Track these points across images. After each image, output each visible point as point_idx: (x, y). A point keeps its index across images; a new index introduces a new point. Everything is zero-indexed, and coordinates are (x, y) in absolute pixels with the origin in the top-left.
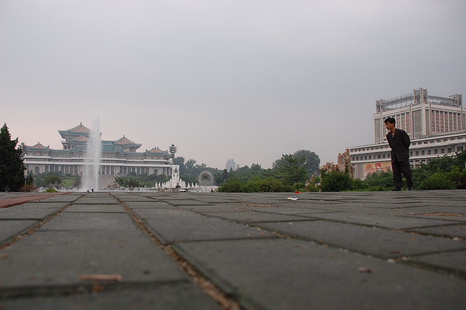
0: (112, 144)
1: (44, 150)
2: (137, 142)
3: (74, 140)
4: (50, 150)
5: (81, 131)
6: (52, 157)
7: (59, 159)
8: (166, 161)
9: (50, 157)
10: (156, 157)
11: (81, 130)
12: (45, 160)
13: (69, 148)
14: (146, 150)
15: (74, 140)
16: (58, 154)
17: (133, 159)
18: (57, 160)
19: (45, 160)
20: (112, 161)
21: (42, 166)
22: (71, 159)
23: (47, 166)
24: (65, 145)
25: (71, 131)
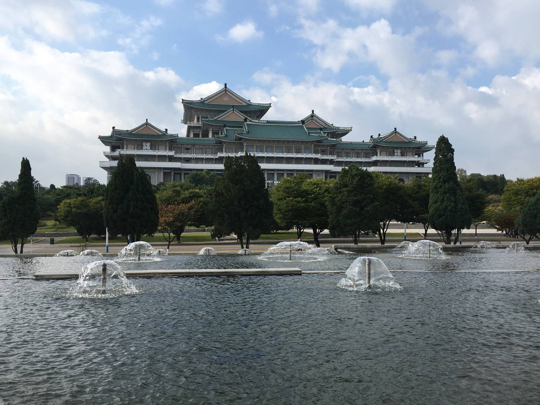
0: (301, 124)
1: (158, 136)
2: (339, 123)
3: (216, 118)
4: (171, 135)
5: (226, 100)
6: (176, 153)
7: (191, 158)
8: (416, 158)
9: (172, 153)
10: (399, 151)
11: (226, 99)
12: (161, 158)
13: (206, 135)
14: (372, 137)
15: (216, 118)
16: (189, 146)
17: (358, 157)
18: (188, 160)
19: (161, 158)
20: (308, 161)
21: (157, 174)
22: (217, 157)
23: (167, 172)
24: (197, 131)
25: (206, 102)
